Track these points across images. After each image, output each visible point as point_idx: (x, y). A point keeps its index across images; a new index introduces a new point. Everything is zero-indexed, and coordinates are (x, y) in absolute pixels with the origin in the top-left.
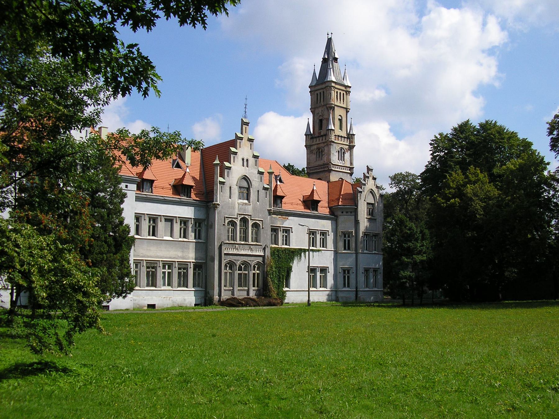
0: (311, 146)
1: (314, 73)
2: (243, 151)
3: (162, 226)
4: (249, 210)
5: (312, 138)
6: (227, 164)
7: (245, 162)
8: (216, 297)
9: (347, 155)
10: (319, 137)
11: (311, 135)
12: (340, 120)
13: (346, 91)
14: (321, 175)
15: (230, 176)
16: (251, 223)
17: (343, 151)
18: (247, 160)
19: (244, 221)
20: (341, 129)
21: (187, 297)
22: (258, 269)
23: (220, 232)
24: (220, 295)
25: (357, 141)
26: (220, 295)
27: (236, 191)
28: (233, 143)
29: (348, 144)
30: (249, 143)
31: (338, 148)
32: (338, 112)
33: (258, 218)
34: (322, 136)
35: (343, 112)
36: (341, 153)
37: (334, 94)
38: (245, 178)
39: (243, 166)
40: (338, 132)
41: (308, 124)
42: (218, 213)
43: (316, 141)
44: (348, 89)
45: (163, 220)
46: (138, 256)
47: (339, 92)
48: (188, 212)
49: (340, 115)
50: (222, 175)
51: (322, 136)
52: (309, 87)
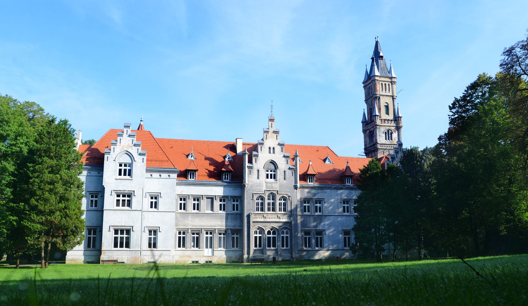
0: (366, 130)
2: (271, 142)
3: (204, 204)
6: (254, 153)
7: (271, 150)
8: (245, 256)
9: (395, 135)
12: (387, 107)
13: (391, 82)
14: (373, 154)
16: (278, 197)
17: (390, 132)
18: (274, 148)
20: (387, 113)
21: (220, 255)
23: (249, 206)
24: (248, 253)
25: (403, 122)
26: (248, 253)
27: (263, 174)
29: (395, 125)
30: (275, 135)
31: (383, 129)
32: (383, 101)
33: (284, 193)
35: (389, 100)
36: (388, 134)
37: (379, 87)
38: (273, 162)
39: (270, 153)
40: (384, 116)
42: (247, 191)
43: (369, 127)
44: (393, 80)
45: (205, 198)
48: (218, 191)
50: (250, 161)
52: (363, 83)
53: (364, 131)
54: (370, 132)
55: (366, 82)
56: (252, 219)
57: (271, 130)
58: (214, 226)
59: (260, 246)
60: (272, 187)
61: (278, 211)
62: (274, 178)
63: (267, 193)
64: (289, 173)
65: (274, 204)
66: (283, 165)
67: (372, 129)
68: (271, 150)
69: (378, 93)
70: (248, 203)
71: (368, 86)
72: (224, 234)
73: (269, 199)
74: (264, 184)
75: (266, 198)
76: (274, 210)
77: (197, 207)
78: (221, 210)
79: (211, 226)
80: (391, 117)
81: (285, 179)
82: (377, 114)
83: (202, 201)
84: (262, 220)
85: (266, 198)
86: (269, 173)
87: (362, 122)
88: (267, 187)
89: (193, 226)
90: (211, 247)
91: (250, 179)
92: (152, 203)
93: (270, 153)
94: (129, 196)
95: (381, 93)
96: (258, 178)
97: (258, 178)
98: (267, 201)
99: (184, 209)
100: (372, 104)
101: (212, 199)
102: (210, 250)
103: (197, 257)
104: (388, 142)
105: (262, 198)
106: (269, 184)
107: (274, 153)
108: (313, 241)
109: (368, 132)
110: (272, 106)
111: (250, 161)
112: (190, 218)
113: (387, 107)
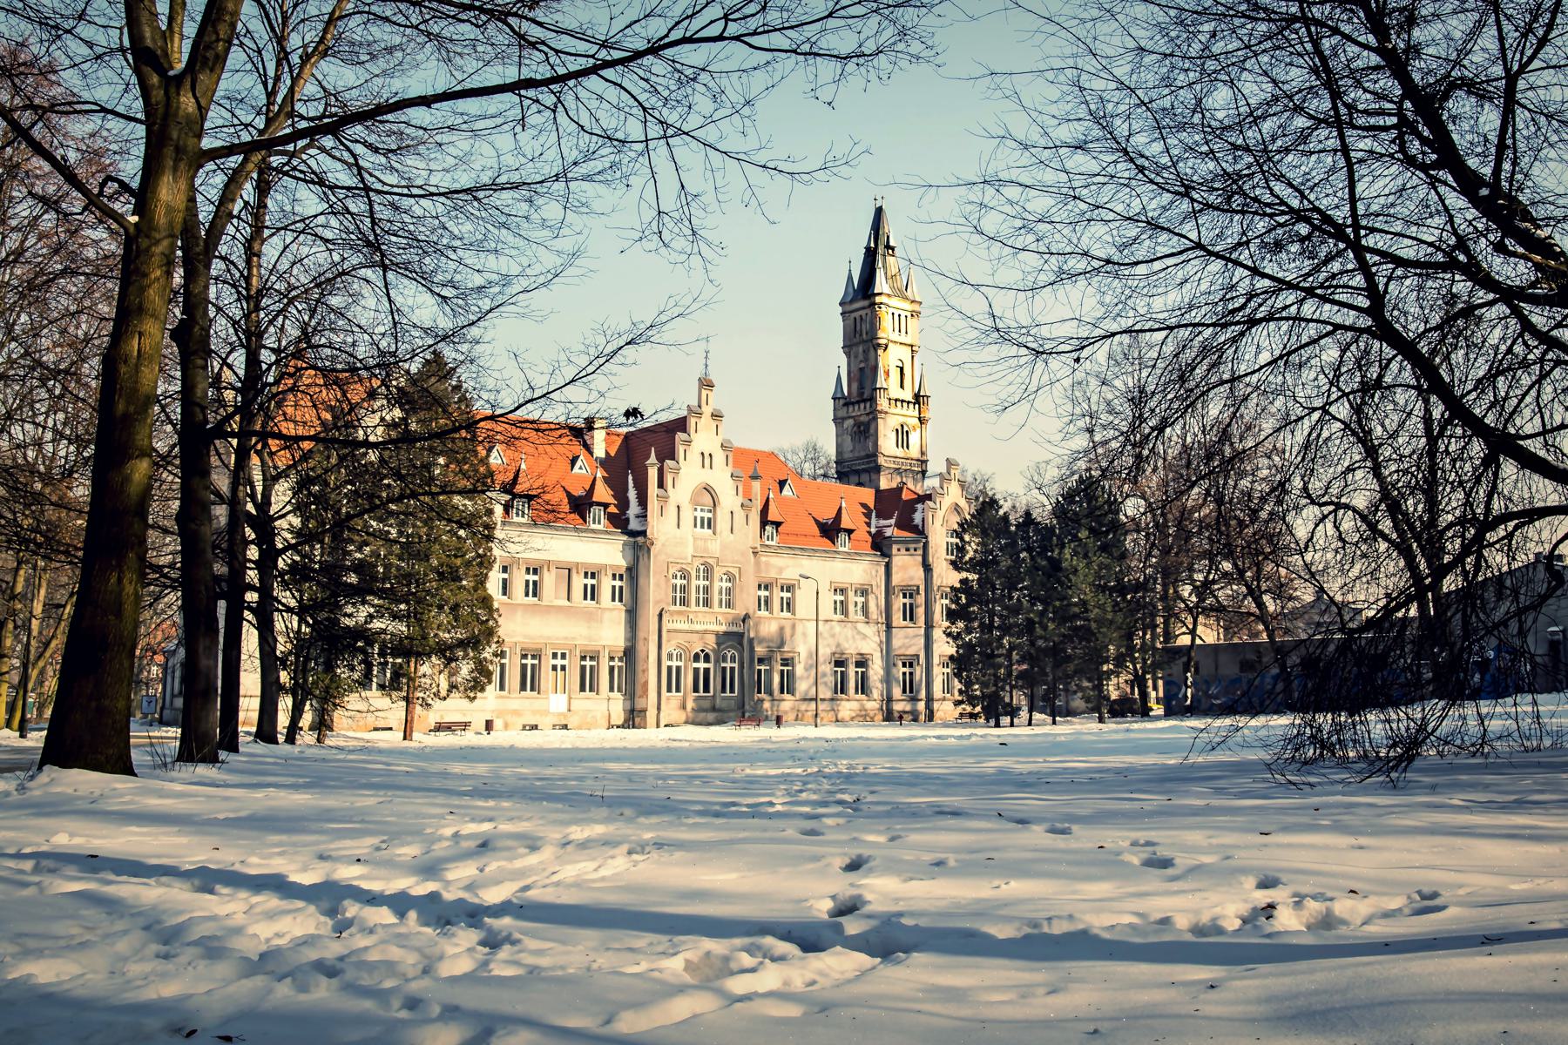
1: (850, 278)
2: (703, 438)
3: (549, 580)
4: (714, 547)
5: (846, 404)
7: (706, 459)
9: (914, 438)
10: (858, 402)
11: (844, 397)
14: (865, 478)
16: (718, 572)
19: (708, 572)
22: (733, 660)
23: (656, 591)
28: (681, 425)
36: (902, 435)
38: (708, 489)
40: (895, 392)
51: (864, 401)
52: (841, 304)
53: (837, 420)
54: (858, 425)
55: (852, 302)
57: (707, 410)
59: (706, 689)
60: (706, 550)
61: (716, 608)
63: (697, 562)
65: (706, 590)
66: (729, 498)
67: (864, 419)
68: (706, 459)
69: (880, 334)
70: (657, 585)
72: (621, 659)
73: (698, 578)
75: (694, 574)
76: (707, 603)
77: (534, 590)
78: (527, 595)
84: (686, 626)
85: (694, 574)
86: (699, 514)
87: (834, 398)
88: (695, 549)
89: (525, 636)
91: (661, 527)
98: (694, 582)
99: (535, 595)
100: (866, 360)
103: (535, 712)
104: (900, 452)
105: (685, 575)
106: (700, 543)
108: (776, 679)
109: (850, 422)
111: (661, 485)
112: (519, 614)
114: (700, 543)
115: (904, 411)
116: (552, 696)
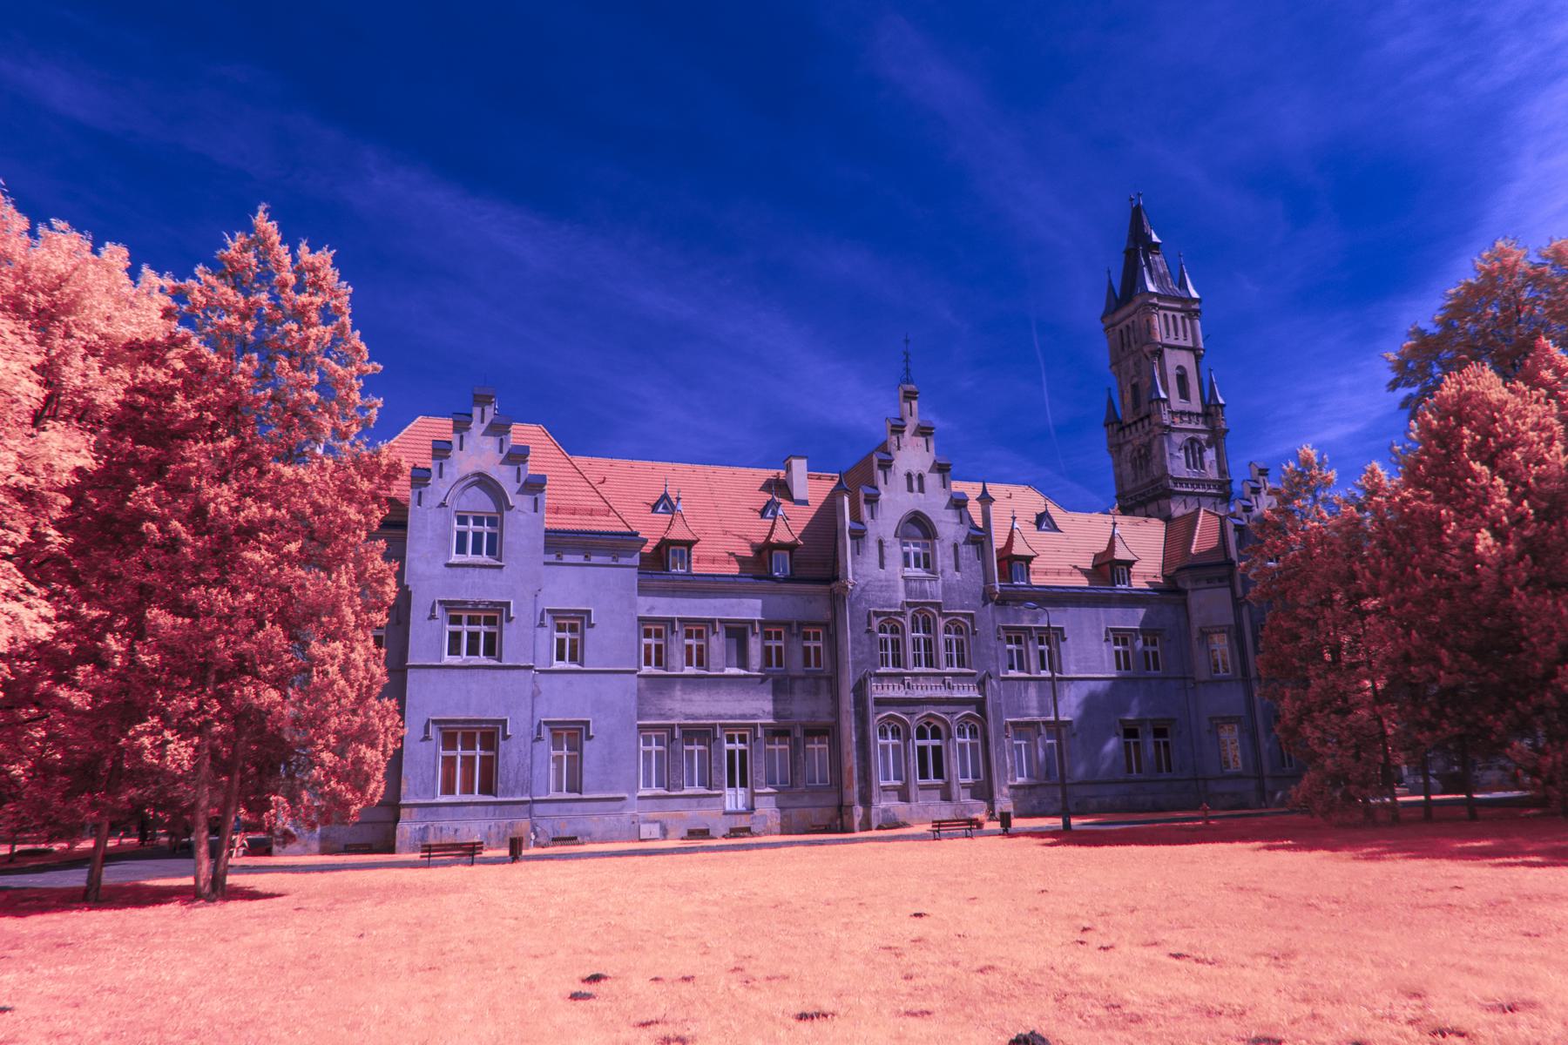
0: (1120, 446)
1: (1111, 288)
4: (935, 590)
7: (915, 482)
9: (1210, 455)
12: (1182, 379)
14: (1152, 507)
15: (879, 516)
17: (1197, 447)
31: (1178, 438)
34: (1142, 420)
35: (1187, 360)
36: (1193, 449)
40: (1177, 403)
41: (1111, 402)
42: (851, 606)
46: (649, 716)
47: (1170, 314)
49: (1179, 367)
51: (1142, 420)
56: (877, 690)
58: (754, 716)
60: (923, 593)
62: (927, 566)
64: (967, 552)
68: (915, 482)
71: (1122, 326)
74: (901, 583)
75: (907, 623)
79: (743, 716)
80: (1195, 405)
81: (957, 568)
82: (1163, 395)
83: (713, 639)
88: (908, 593)
90: (743, 784)
91: (859, 569)
92: (561, 642)
93: (910, 490)
94: (490, 621)
95: (1165, 341)
96: (882, 566)
97: (882, 566)
98: (910, 635)
101: (737, 633)
102: (741, 791)
106: (913, 585)
107: (922, 490)
110: (907, 354)
113: (1182, 379)
114: (913, 585)
115: (1192, 426)
116: (728, 792)
